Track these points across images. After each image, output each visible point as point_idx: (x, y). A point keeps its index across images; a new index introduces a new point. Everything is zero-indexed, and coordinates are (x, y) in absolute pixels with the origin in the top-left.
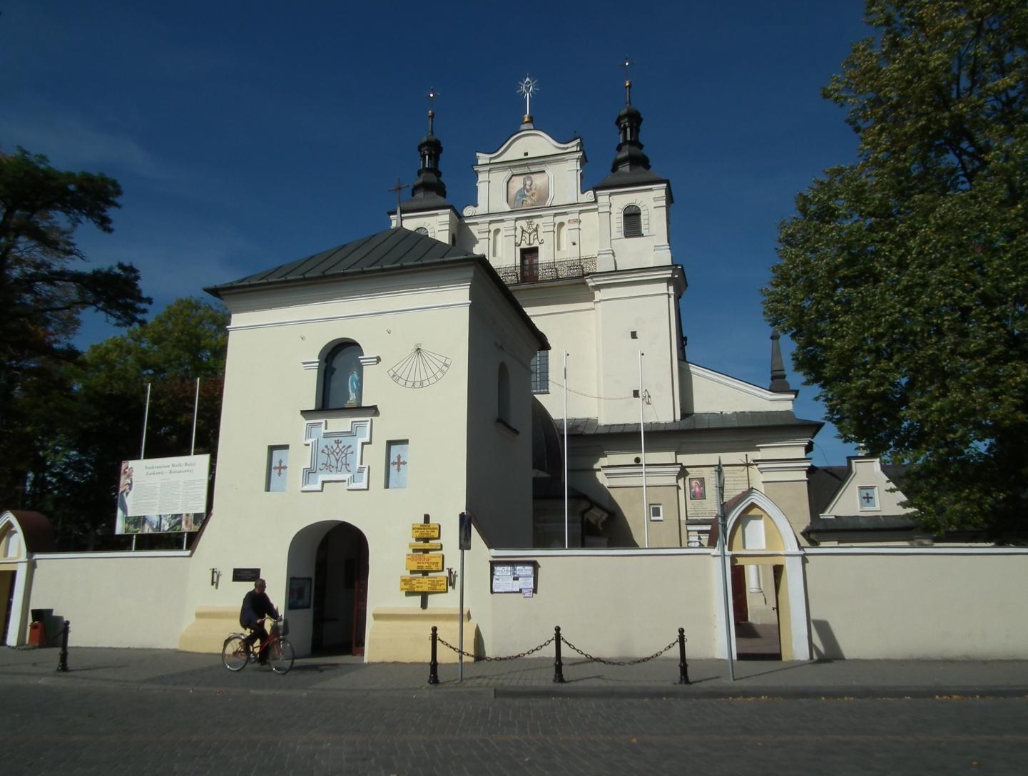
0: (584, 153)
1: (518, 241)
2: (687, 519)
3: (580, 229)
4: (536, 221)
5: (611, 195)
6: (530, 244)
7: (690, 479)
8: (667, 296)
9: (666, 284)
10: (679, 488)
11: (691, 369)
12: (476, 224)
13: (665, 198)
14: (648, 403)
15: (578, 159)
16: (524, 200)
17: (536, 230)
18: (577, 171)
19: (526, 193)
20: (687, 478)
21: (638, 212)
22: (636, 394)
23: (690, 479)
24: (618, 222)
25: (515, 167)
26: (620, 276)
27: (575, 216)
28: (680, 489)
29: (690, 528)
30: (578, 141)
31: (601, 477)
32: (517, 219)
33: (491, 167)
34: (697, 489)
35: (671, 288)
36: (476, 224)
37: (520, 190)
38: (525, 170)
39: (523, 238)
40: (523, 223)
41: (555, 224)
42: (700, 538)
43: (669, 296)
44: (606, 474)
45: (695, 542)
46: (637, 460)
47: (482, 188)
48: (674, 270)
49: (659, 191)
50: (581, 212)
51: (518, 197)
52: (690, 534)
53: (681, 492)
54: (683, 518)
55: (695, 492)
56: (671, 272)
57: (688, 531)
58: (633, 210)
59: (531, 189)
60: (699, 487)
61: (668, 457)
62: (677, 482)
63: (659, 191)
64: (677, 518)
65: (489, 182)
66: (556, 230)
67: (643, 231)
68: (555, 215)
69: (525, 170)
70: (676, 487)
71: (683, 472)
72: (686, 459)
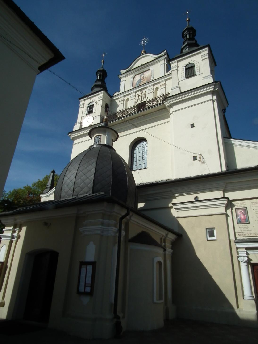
0: (168, 56)
1: (136, 101)
2: (236, 239)
3: (166, 88)
4: (144, 91)
5: (178, 62)
6: (142, 101)
7: (236, 209)
8: (212, 101)
9: (211, 95)
10: (227, 216)
11: (233, 142)
12: (118, 98)
13: (208, 54)
14: (203, 163)
15: (165, 59)
16: (140, 84)
17: (145, 94)
18: (165, 64)
19: (141, 81)
20: (234, 209)
21: (193, 65)
22: (195, 158)
23: (236, 209)
24: (182, 72)
25: (136, 71)
26: (183, 96)
27: (164, 83)
28: (229, 216)
29: (239, 245)
30: (165, 51)
31: (174, 212)
32: (136, 92)
33: (126, 74)
34: (242, 216)
35: (215, 98)
36: (118, 98)
37: (139, 80)
38: (141, 71)
39: (139, 99)
40: (139, 93)
41: (154, 89)
42: (247, 254)
43: (213, 101)
44: (176, 209)
45: (244, 256)
46: (196, 198)
47: (122, 84)
48: (215, 85)
49: (205, 52)
50: (166, 80)
51: (138, 83)
52: (239, 250)
53: (230, 219)
54: (232, 238)
55: (240, 218)
56: (213, 86)
57: (237, 248)
58: (190, 66)
59: (143, 78)
60: (244, 215)
61: (219, 194)
62: (226, 211)
63: (205, 52)
64: (227, 237)
65: (125, 81)
66: (154, 91)
67: (197, 73)
68: (154, 85)
69: (141, 71)
70: (225, 215)
71: (230, 204)
72: (232, 195)
